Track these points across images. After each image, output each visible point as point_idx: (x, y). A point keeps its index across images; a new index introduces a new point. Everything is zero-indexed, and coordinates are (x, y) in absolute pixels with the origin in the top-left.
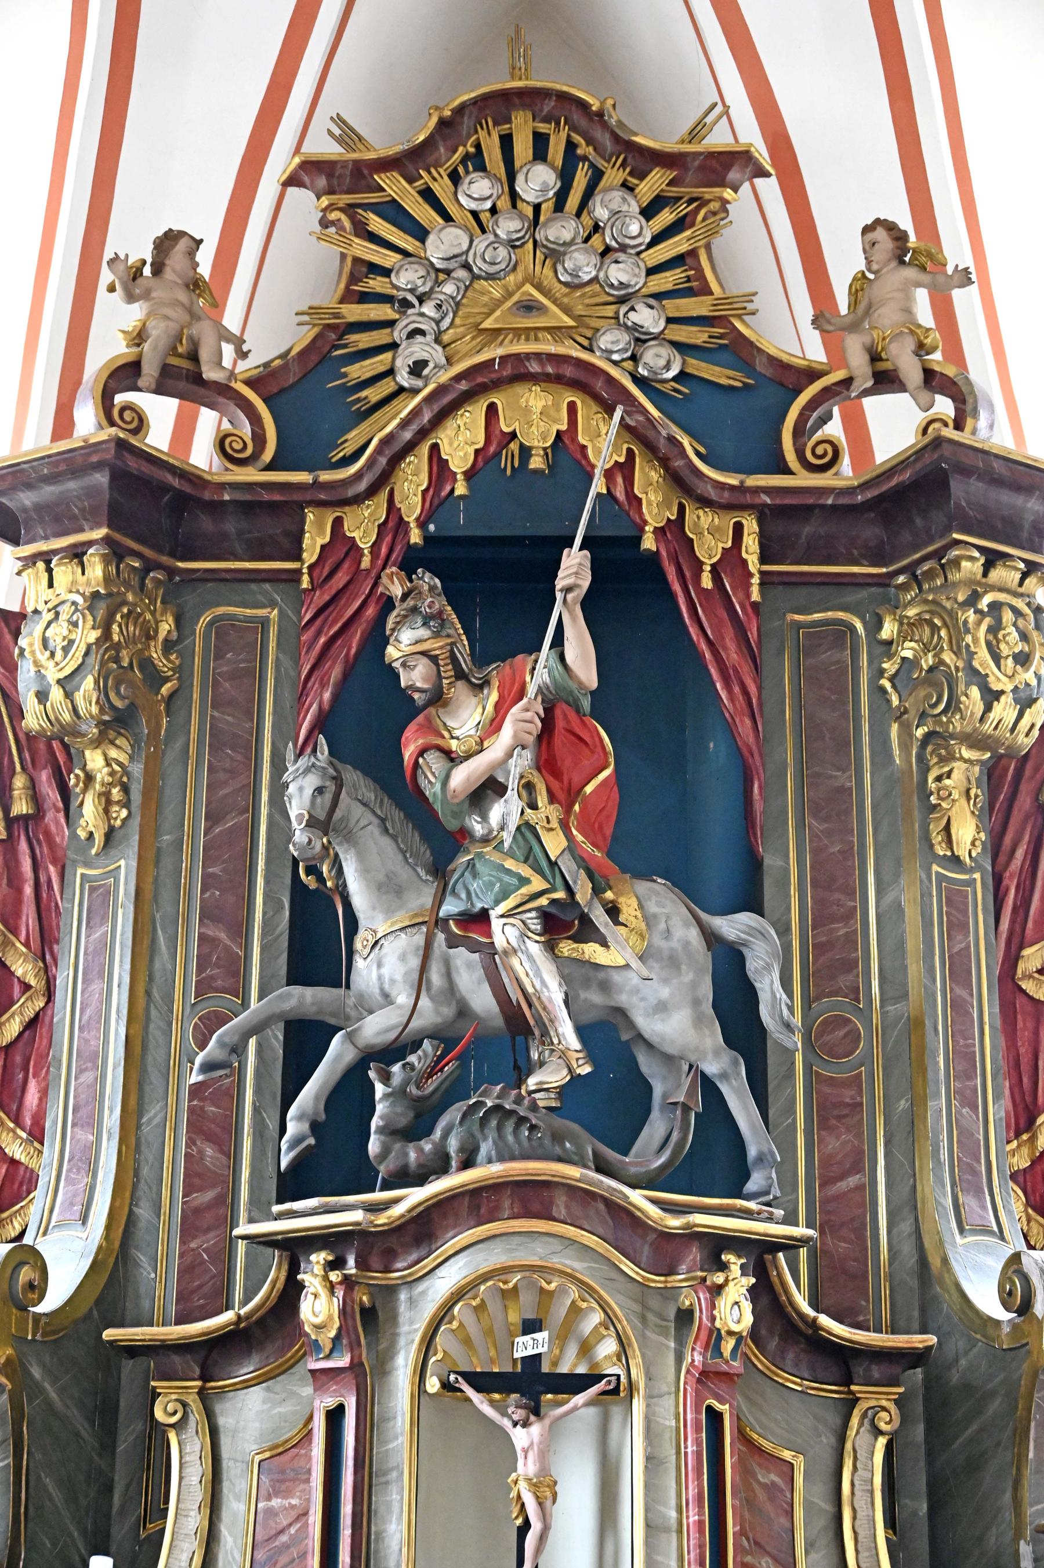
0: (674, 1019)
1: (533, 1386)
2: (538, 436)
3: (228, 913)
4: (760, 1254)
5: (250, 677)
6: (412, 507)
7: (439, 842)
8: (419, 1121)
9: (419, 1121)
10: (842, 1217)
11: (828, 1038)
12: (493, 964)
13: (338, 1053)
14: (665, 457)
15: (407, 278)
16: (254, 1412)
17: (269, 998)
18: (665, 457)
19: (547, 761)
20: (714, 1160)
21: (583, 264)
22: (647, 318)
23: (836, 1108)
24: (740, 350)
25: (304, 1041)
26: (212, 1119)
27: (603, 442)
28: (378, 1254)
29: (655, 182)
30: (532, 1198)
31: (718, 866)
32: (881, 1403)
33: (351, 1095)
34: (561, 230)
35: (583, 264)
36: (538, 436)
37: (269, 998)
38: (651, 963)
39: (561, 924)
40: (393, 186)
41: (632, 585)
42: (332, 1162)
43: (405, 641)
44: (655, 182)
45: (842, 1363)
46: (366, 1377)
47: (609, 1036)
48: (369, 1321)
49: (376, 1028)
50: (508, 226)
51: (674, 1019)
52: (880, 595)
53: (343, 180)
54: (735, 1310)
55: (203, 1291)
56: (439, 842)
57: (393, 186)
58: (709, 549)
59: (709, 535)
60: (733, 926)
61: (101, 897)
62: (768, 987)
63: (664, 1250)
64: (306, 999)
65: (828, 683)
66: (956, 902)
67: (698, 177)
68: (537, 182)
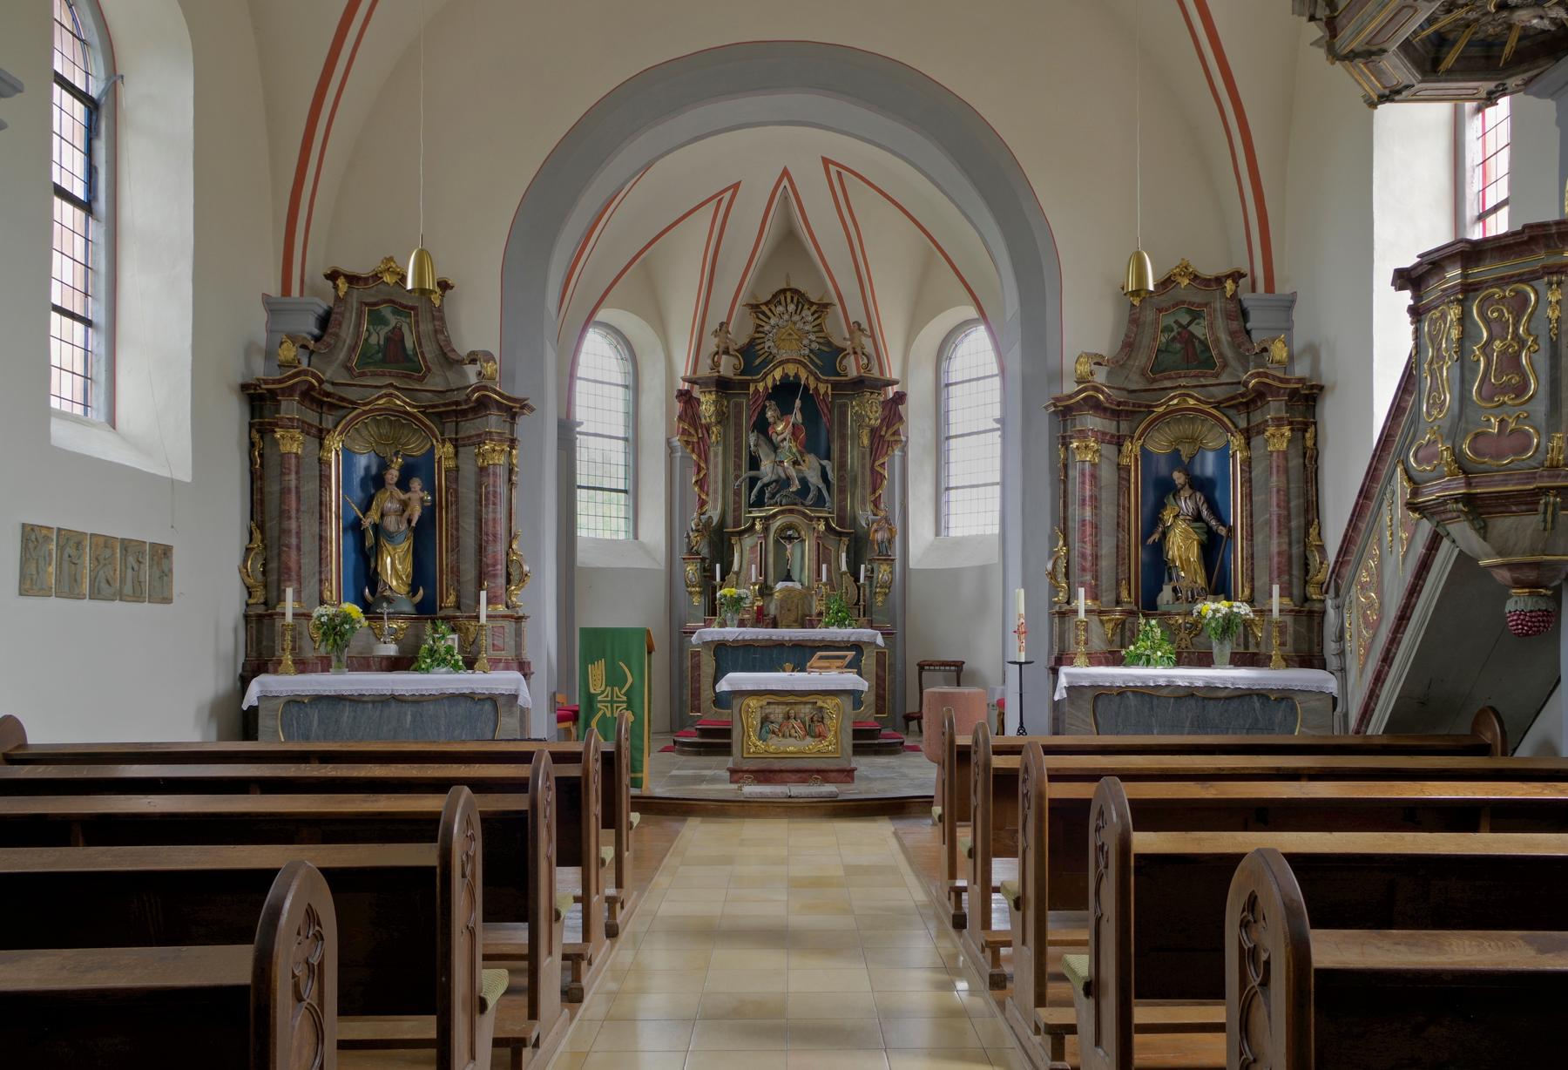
0: (814, 479)
1: (790, 539)
2: (792, 374)
3: (738, 456)
4: (826, 519)
5: (740, 412)
6: (770, 385)
7: (775, 448)
8: (773, 496)
9: (773, 496)
10: (842, 509)
11: (841, 478)
12: (784, 469)
13: (759, 484)
14: (815, 375)
15: (767, 328)
16: (748, 541)
17: (746, 474)
18: (815, 375)
19: (793, 434)
20: (820, 501)
21: (800, 325)
22: (813, 337)
23: (842, 491)
24: (829, 344)
25: (753, 481)
26: (737, 493)
27: (803, 375)
28: (767, 520)
29: (814, 308)
30: (791, 511)
31: (823, 450)
32: (845, 540)
33: (762, 492)
34: (796, 318)
35: (800, 325)
36: (792, 374)
37: (746, 474)
38: (811, 469)
39: (796, 463)
40: (764, 308)
41: (810, 400)
42: (759, 503)
43: (769, 414)
44: (814, 308)
45: (840, 534)
46: (766, 538)
47: (804, 481)
48: (766, 529)
49: (766, 480)
50: (786, 317)
51: (814, 479)
52: (852, 397)
53: (755, 307)
54: (822, 527)
55: (737, 523)
56: (775, 448)
57: (764, 308)
58: (822, 391)
59: (822, 388)
60: (825, 462)
61: (716, 455)
62: (830, 475)
63: (811, 519)
64: (753, 473)
65: (843, 415)
66: (864, 454)
67: (823, 307)
68: (792, 307)
